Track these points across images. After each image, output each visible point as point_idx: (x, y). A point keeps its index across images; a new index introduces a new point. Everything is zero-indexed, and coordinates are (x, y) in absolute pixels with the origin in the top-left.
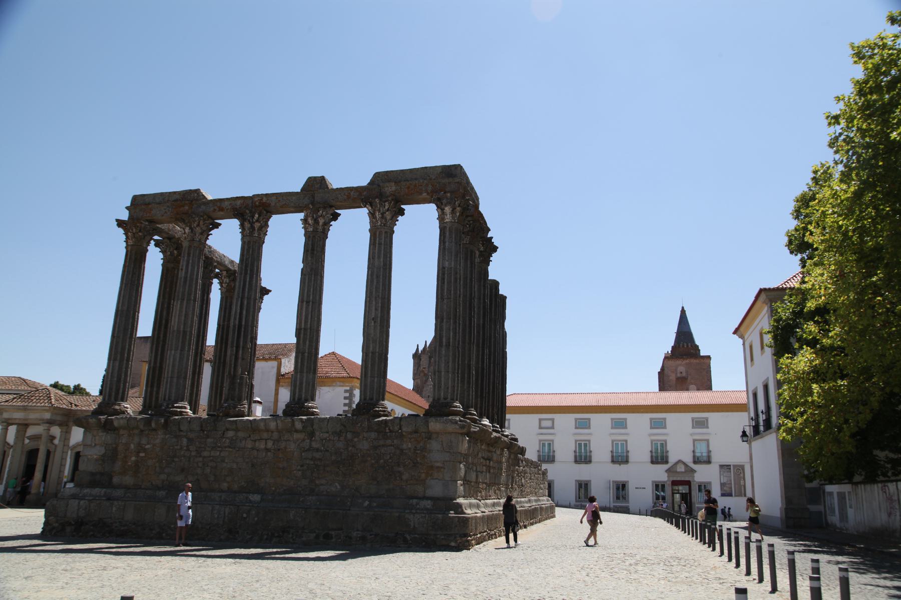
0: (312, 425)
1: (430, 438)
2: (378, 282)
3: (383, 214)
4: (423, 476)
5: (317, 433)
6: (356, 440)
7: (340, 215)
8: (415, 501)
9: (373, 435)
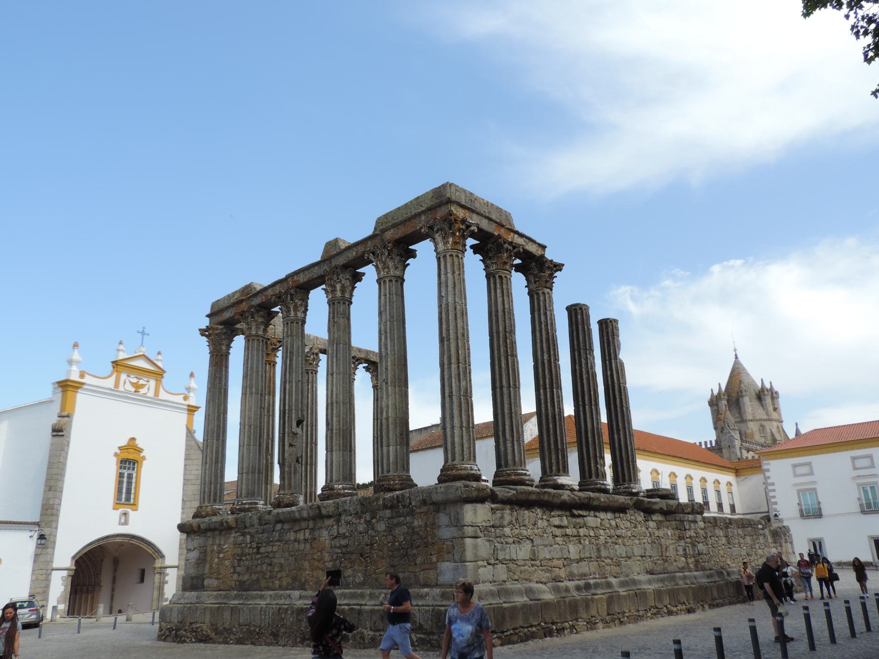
0: (338, 508)
1: (438, 511)
2: (386, 338)
3: (384, 263)
4: (434, 559)
5: (343, 517)
6: (374, 521)
7: (364, 274)
8: (426, 590)
9: (388, 513)
